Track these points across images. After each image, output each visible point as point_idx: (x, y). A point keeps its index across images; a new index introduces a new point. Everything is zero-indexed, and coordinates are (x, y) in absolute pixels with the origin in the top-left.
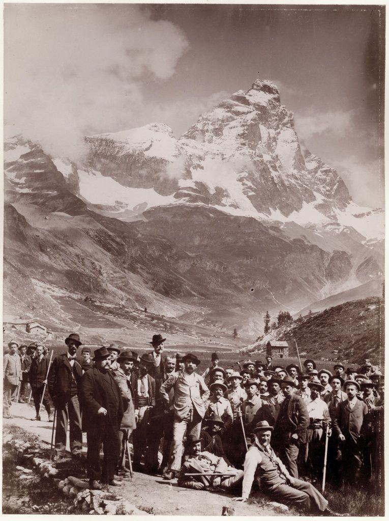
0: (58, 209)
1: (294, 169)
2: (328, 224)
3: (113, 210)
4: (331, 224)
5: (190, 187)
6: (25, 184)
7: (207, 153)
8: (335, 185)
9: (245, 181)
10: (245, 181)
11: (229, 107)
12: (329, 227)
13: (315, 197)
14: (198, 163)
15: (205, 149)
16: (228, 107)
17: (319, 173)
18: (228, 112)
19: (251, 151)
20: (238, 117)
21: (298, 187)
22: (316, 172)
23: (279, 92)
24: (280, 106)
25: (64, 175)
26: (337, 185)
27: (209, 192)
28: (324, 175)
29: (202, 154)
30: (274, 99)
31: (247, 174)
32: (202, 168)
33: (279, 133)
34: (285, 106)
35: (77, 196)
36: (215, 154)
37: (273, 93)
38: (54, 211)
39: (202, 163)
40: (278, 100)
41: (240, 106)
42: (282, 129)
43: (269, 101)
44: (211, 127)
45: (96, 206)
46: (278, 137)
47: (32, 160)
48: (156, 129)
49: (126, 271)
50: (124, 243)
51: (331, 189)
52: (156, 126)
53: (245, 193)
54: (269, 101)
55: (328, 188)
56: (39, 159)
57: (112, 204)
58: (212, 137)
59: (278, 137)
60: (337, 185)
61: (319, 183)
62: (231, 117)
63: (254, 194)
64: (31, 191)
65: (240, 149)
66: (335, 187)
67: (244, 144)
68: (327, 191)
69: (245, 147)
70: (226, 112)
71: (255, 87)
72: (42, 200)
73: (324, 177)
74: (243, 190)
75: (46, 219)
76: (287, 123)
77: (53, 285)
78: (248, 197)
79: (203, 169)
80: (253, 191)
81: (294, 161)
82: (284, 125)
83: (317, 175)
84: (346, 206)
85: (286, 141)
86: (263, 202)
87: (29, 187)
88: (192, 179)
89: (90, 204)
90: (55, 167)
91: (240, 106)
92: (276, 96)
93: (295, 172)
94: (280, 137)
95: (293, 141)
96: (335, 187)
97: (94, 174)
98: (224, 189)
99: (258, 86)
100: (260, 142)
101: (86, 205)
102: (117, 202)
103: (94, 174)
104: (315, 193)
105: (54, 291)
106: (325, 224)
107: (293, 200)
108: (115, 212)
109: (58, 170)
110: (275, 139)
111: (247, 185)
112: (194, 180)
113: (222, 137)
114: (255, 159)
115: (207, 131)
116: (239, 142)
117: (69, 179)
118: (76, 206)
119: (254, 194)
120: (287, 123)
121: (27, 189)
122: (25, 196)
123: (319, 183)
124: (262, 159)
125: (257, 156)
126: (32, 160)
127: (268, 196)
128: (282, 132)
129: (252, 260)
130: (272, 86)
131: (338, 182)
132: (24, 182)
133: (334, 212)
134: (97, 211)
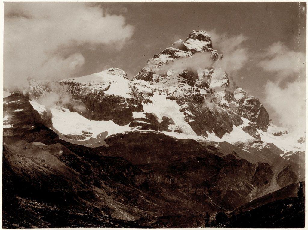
0: (35, 140)
1: (225, 100)
2: (254, 142)
3: (80, 138)
4: (256, 142)
5: (142, 118)
6: (7, 121)
7: (154, 91)
8: (258, 111)
9: (186, 111)
10: (186, 111)
11: (171, 53)
12: (255, 144)
13: (242, 121)
14: (148, 98)
15: (153, 87)
16: (170, 54)
17: (245, 102)
18: (170, 57)
19: (190, 87)
21: (229, 114)
23: (211, 40)
24: (212, 51)
25: (39, 113)
26: (260, 111)
27: (157, 121)
28: (249, 104)
29: (151, 91)
30: (208, 45)
31: (187, 106)
32: (151, 102)
33: (212, 72)
34: (216, 51)
35: (50, 129)
36: (161, 91)
37: (207, 41)
38: (32, 142)
39: (151, 98)
40: (210, 46)
41: (180, 52)
43: (204, 47)
45: (66, 136)
46: (212, 75)
47: (13, 102)
48: (113, 72)
49: (93, 186)
50: (90, 165)
51: (255, 114)
52: (113, 71)
53: (187, 120)
54: (204, 47)
55: (253, 114)
56: (18, 100)
57: (79, 133)
58: (159, 77)
60: (260, 111)
61: (245, 110)
63: (194, 121)
64: (12, 126)
65: (181, 86)
66: (258, 113)
67: (184, 82)
69: (186, 84)
71: (192, 36)
72: (22, 134)
73: (249, 105)
74: (185, 118)
75: (26, 148)
77: (34, 200)
78: (189, 123)
79: (152, 103)
80: (193, 119)
83: (244, 104)
84: (267, 128)
86: (201, 127)
87: (11, 124)
88: (143, 111)
89: (61, 135)
90: (31, 107)
91: (180, 52)
92: (209, 43)
93: (226, 102)
94: (213, 75)
95: (224, 78)
96: (258, 113)
97: (64, 111)
98: (169, 118)
99: (194, 36)
100: (197, 80)
101: (58, 135)
102: (83, 132)
103: (64, 111)
104: (243, 119)
105: (35, 205)
106: (251, 142)
107: (225, 124)
108: (82, 140)
109: (35, 109)
110: (209, 77)
111: (188, 114)
112: (145, 112)
113: (167, 78)
114: (193, 93)
116: (180, 80)
117: (43, 116)
118: (51, 137)
119: (194, 121)
121: (9, 125)
122: (8, 131)
123: (245, 110)
124: (199, 93)
125: (195, 91)
126: (13, 102)
127: (205, 122)
129: (193, 173)
130: (205, 35)
131: (260, 108)
132: (7, 120)
133: (258, 132)
134: (68, 140)
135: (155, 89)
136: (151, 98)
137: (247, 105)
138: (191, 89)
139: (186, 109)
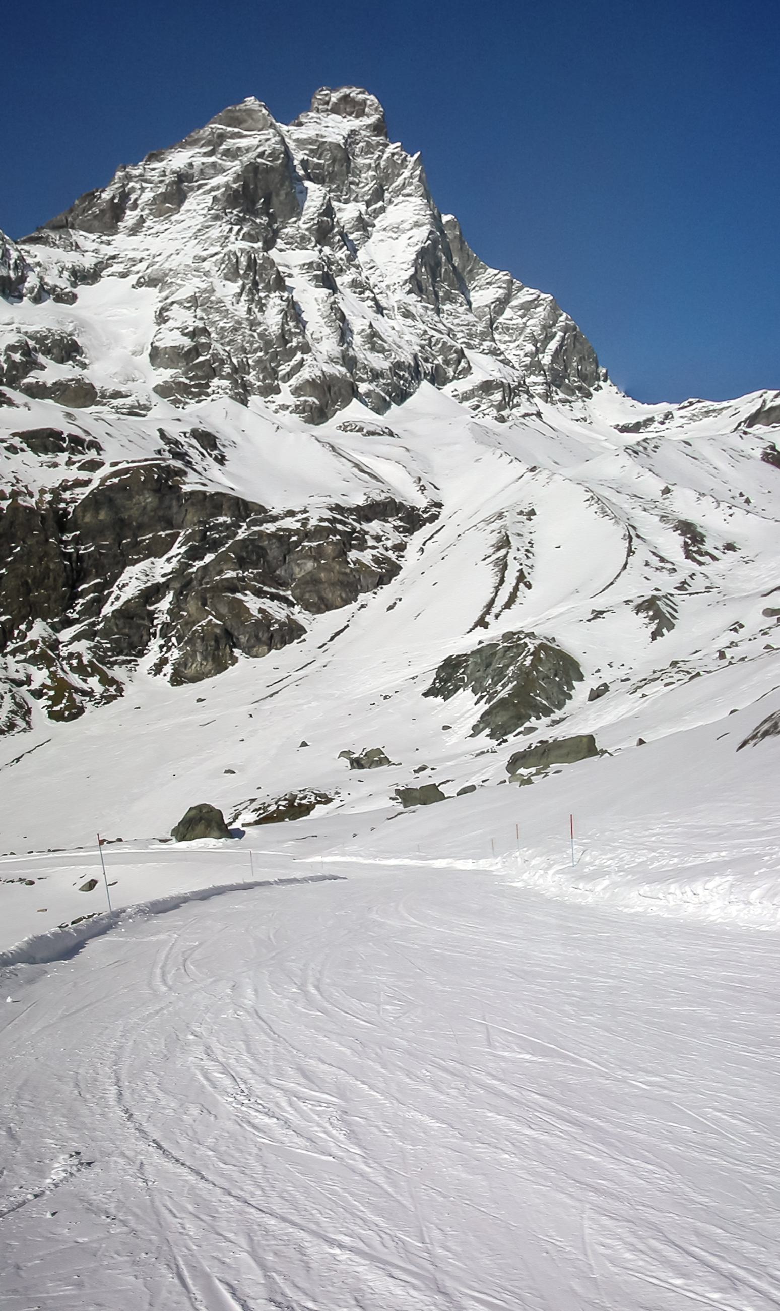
8: (550, 338)
15: (109, 251)
17: (508, 313)
20: (234, 164)
22: (501, 312)
26: (558, 338)
28: (522, 317)
33: (383, 209)
42: (390, 202)
44: (148, 195)
59: (376, 222)
60: (558, 338)
61: (507, 338)
62: (214, 165)
66: (553, 345)
68: (526, 355)
70: (206, 154)
76: (404, 186)
81: (412, 271)
82: (398, 192)
85: (397, 229)
95: (417, 225)
96: (553, 345)
113: (174, 218)
114: (231, 247)
115: (135, 206)
120: (404, 186)
128: (390, 208)
135: (114, 257)
136: (82, 290)
137: (514, 322)
138: (231, 230)
139: (180, 303)
